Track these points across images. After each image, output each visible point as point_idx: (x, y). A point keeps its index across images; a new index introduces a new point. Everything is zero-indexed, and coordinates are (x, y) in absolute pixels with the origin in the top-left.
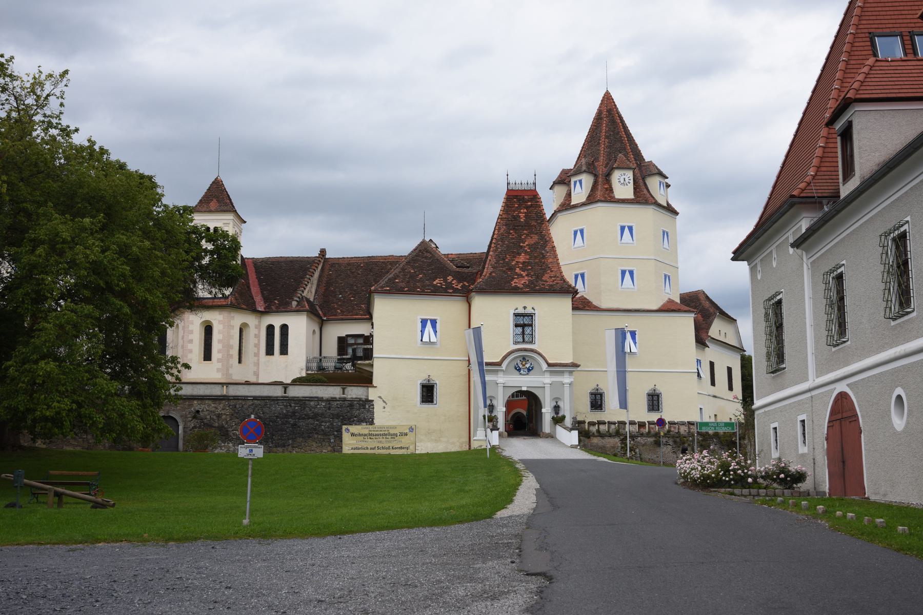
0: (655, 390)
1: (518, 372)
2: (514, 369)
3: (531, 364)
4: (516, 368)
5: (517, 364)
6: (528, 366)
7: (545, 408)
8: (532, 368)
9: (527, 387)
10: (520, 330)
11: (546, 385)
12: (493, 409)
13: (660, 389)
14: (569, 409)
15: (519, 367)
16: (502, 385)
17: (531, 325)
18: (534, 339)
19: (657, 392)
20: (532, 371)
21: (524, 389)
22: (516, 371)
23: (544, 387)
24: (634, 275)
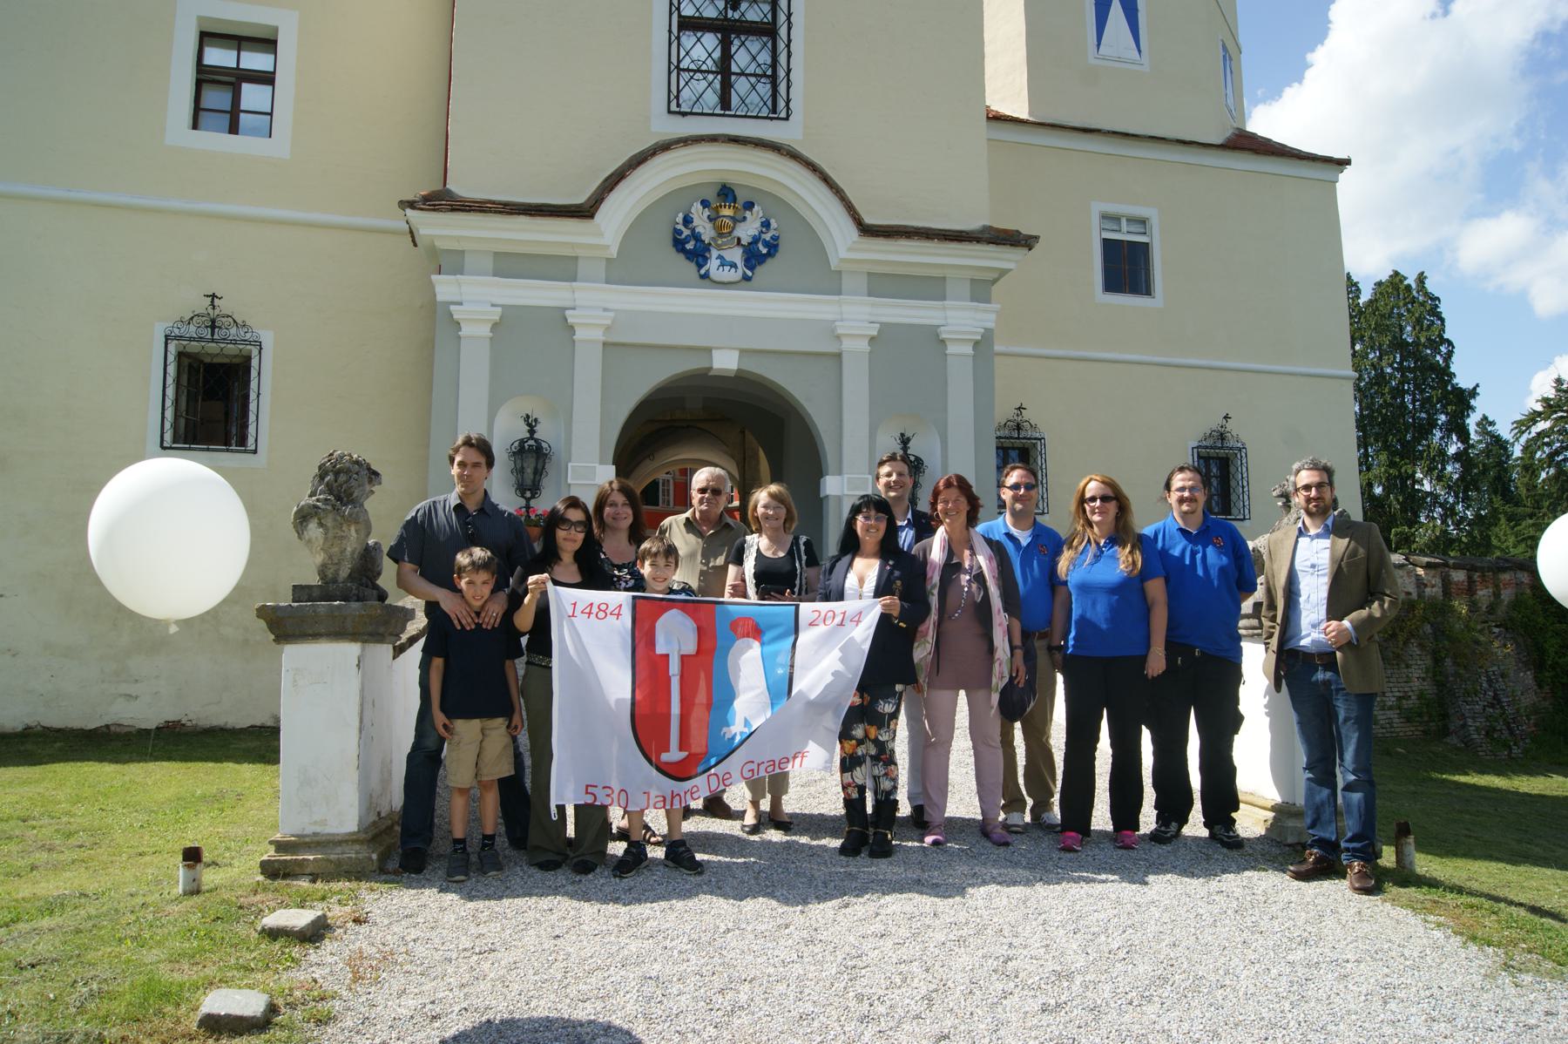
0: (1222, 437)
1: (692, 266)
2: (669, 241)
3: (766, 224)
4: (679, 244)
5: (687, 221)
6: (747, 230)
7: (840, 473)
8: (773, 247)
9: (744, 352)
10: (703, 48)
12: (539, 473)
13: (1239, 430)
15: (696, 237)
17: (767, 31)
18: (783, 59)
19: (1232, 443)
20: (770, 264)
21: (726, 362)
22: (681, 257)
23: (838, 356)
24: (1139, 15)
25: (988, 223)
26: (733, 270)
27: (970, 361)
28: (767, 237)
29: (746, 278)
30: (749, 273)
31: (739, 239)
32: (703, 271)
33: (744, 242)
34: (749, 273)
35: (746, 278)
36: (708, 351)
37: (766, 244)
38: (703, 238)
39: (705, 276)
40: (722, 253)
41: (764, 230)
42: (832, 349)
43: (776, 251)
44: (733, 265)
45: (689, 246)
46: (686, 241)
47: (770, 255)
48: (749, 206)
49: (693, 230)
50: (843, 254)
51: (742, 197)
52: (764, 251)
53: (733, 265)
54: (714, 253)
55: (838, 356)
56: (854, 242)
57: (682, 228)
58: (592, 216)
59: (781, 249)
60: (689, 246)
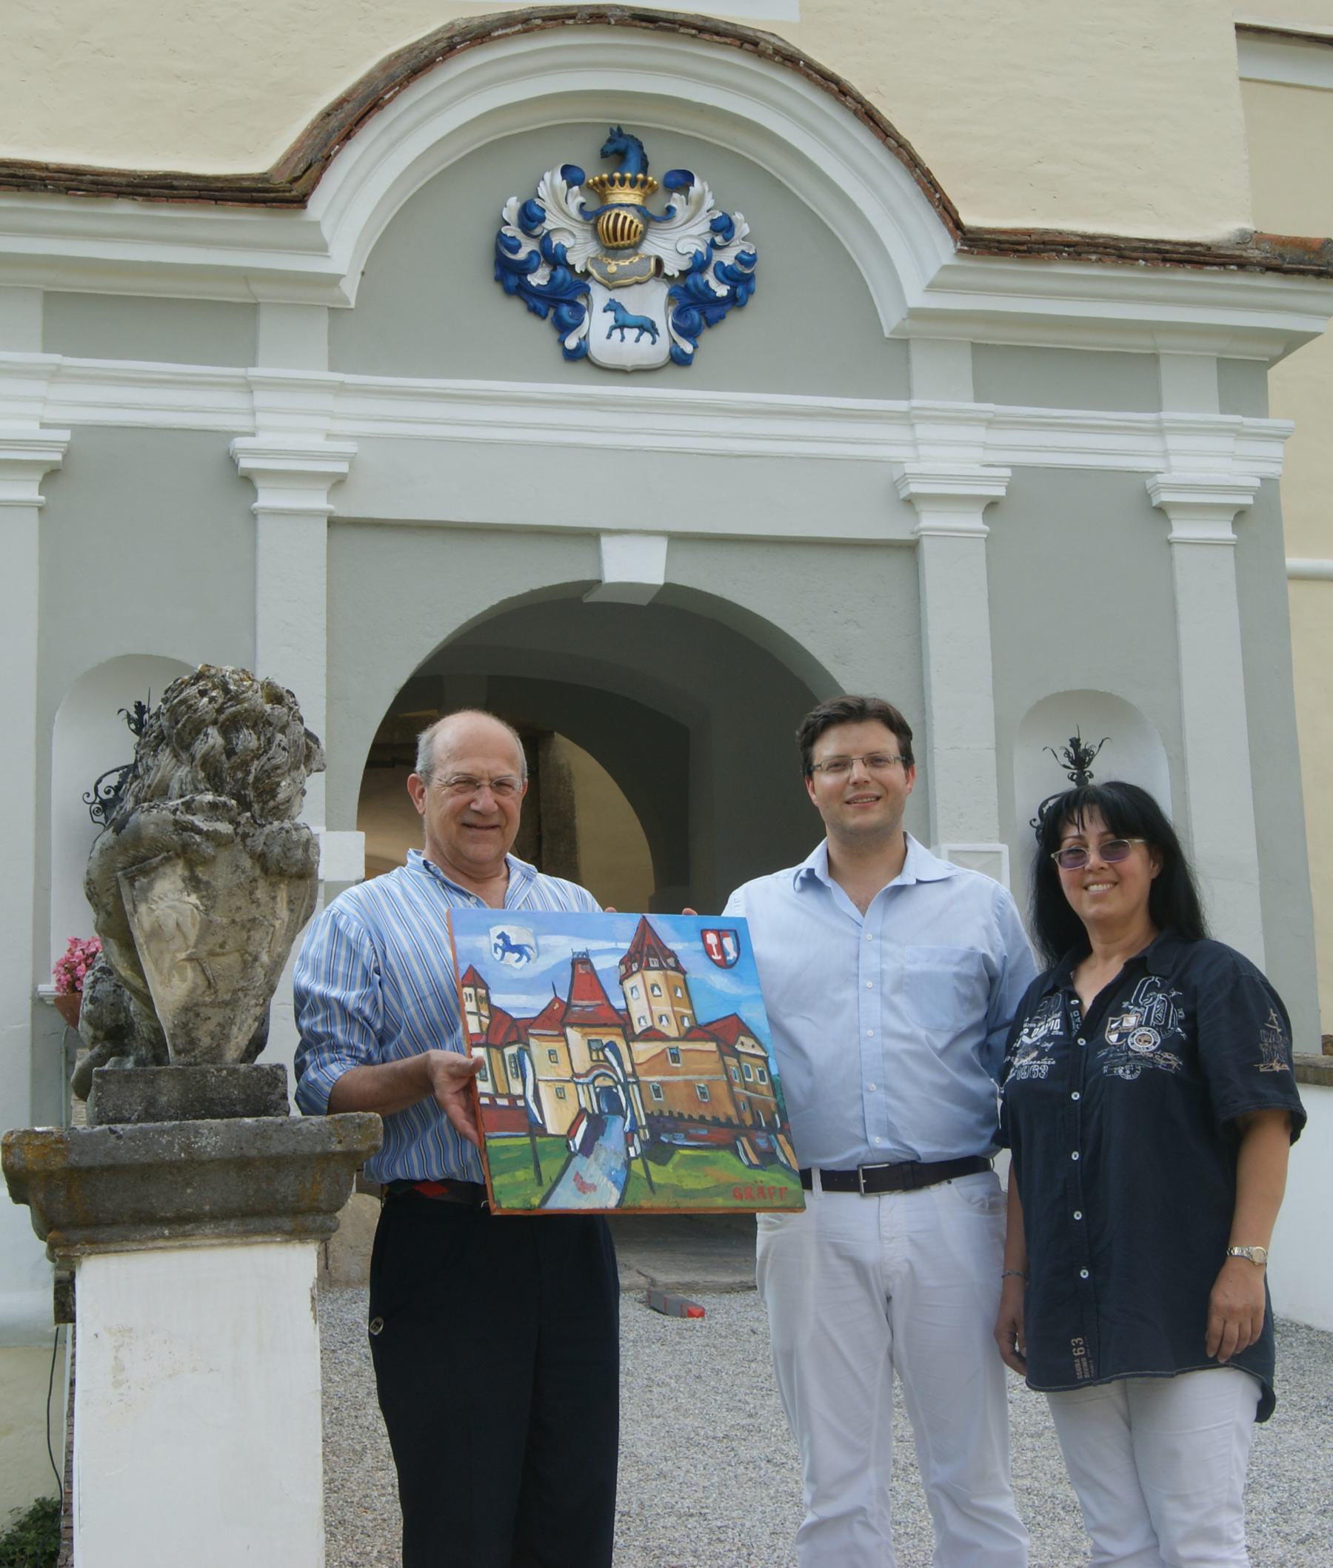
1: (542, 330)
2: (487, 270)
3: (723, 227)
5: (530, 217)
9: (677, 539)
11: (930, 520)
14: (1250, 852)
15: (555, 258)
16: (318, 501)
20: (735, 326)
22: (516, 308)
23: (911, 548)
25: (1250, 227)
26: (647, 337)
27: (1227, 559)
28: (728, 257)
29: (679, 360)
30: (687, 347)
31: (659, 263)
32: (571, 342)
33: (671, 268)
34: (687, 347)
35: (679, 360)
36: (591, 536)
37: (726, 275)
38: (571, 259)
39: (579, 355)
40: (619, 296)
41: (719, 239)
42: (898, 531)
43: (750, 292)
44: (647, 327)
45: (538, 278)
46: (523, 269)
47: (734, 301)
48: (681, 181)
49: (545, 240)
50: (917, 298)
51: (662, 163)
52: (722, 291)
53: (647, 327)
54: (599, 296)
55: (911, 548)
56: (945, 268)
57: (520, 236)
58: (300, 202)
59: (760, 284)
60: (538, 278)
